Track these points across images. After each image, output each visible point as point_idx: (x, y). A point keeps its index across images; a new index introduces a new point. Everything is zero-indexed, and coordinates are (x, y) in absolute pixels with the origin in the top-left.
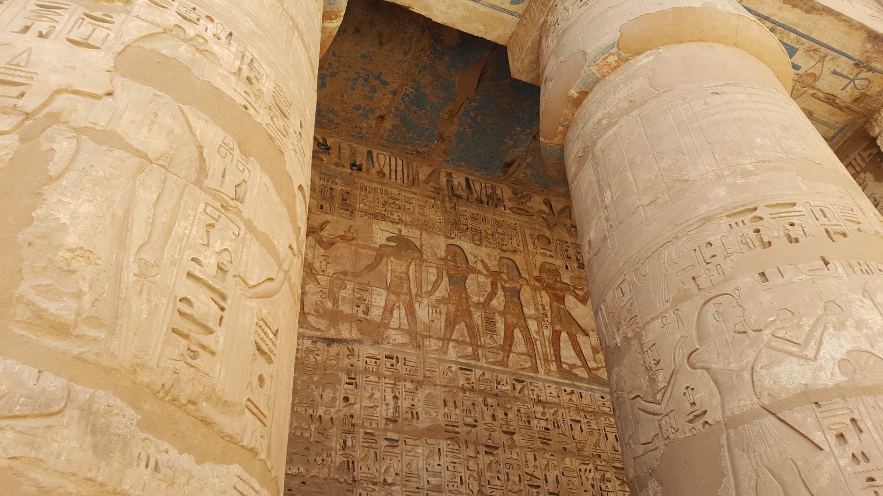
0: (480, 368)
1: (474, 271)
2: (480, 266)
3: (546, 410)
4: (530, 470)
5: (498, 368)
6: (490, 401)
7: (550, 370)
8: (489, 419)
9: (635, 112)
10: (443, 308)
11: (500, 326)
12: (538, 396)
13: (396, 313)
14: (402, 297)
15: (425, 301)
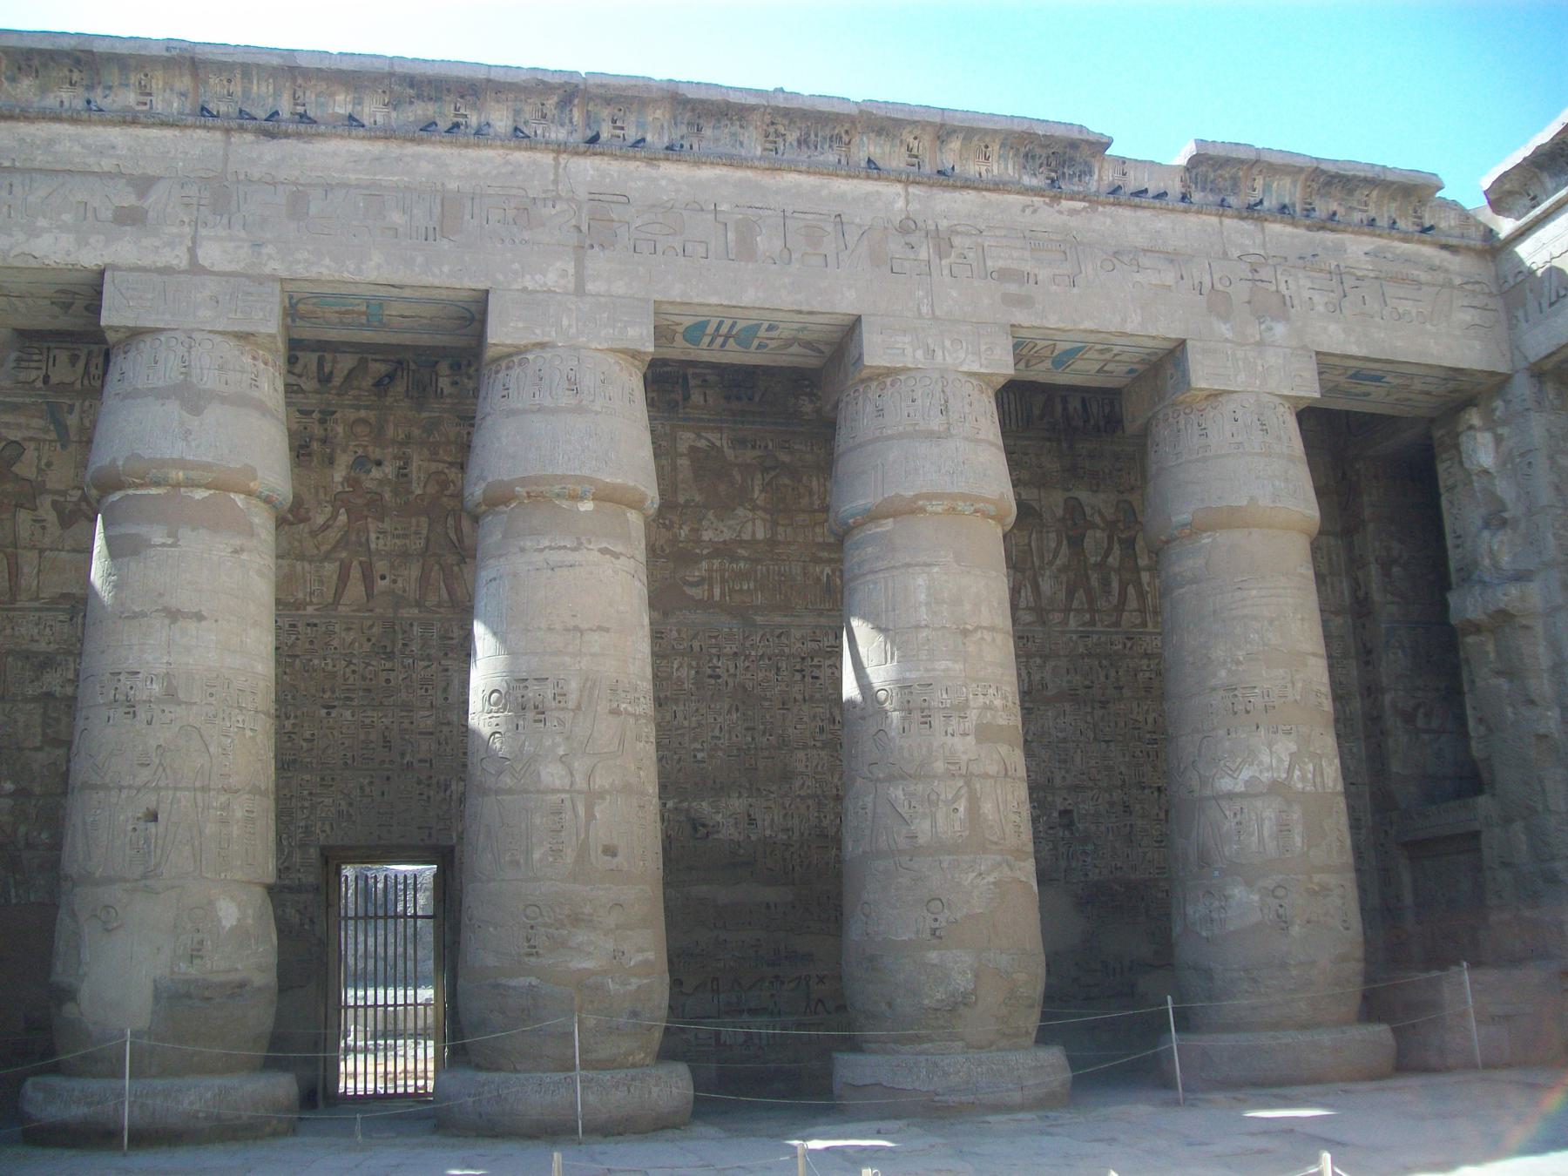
0: (1097, 633)
1: (1094, 526)
2: (1097, 519)
3: (1151, 662)
4: (1134, 716)
5: (1113, 630)
6: (1104, 662)
7: (1157, 622)
8: (1102, 679)
9: (1194, 586)
10: (1064, 578)
11: (1115, 585)
12: (1145, 650)
13: (1023, 594)
14: (1027, 574)
15: (1048, 573)
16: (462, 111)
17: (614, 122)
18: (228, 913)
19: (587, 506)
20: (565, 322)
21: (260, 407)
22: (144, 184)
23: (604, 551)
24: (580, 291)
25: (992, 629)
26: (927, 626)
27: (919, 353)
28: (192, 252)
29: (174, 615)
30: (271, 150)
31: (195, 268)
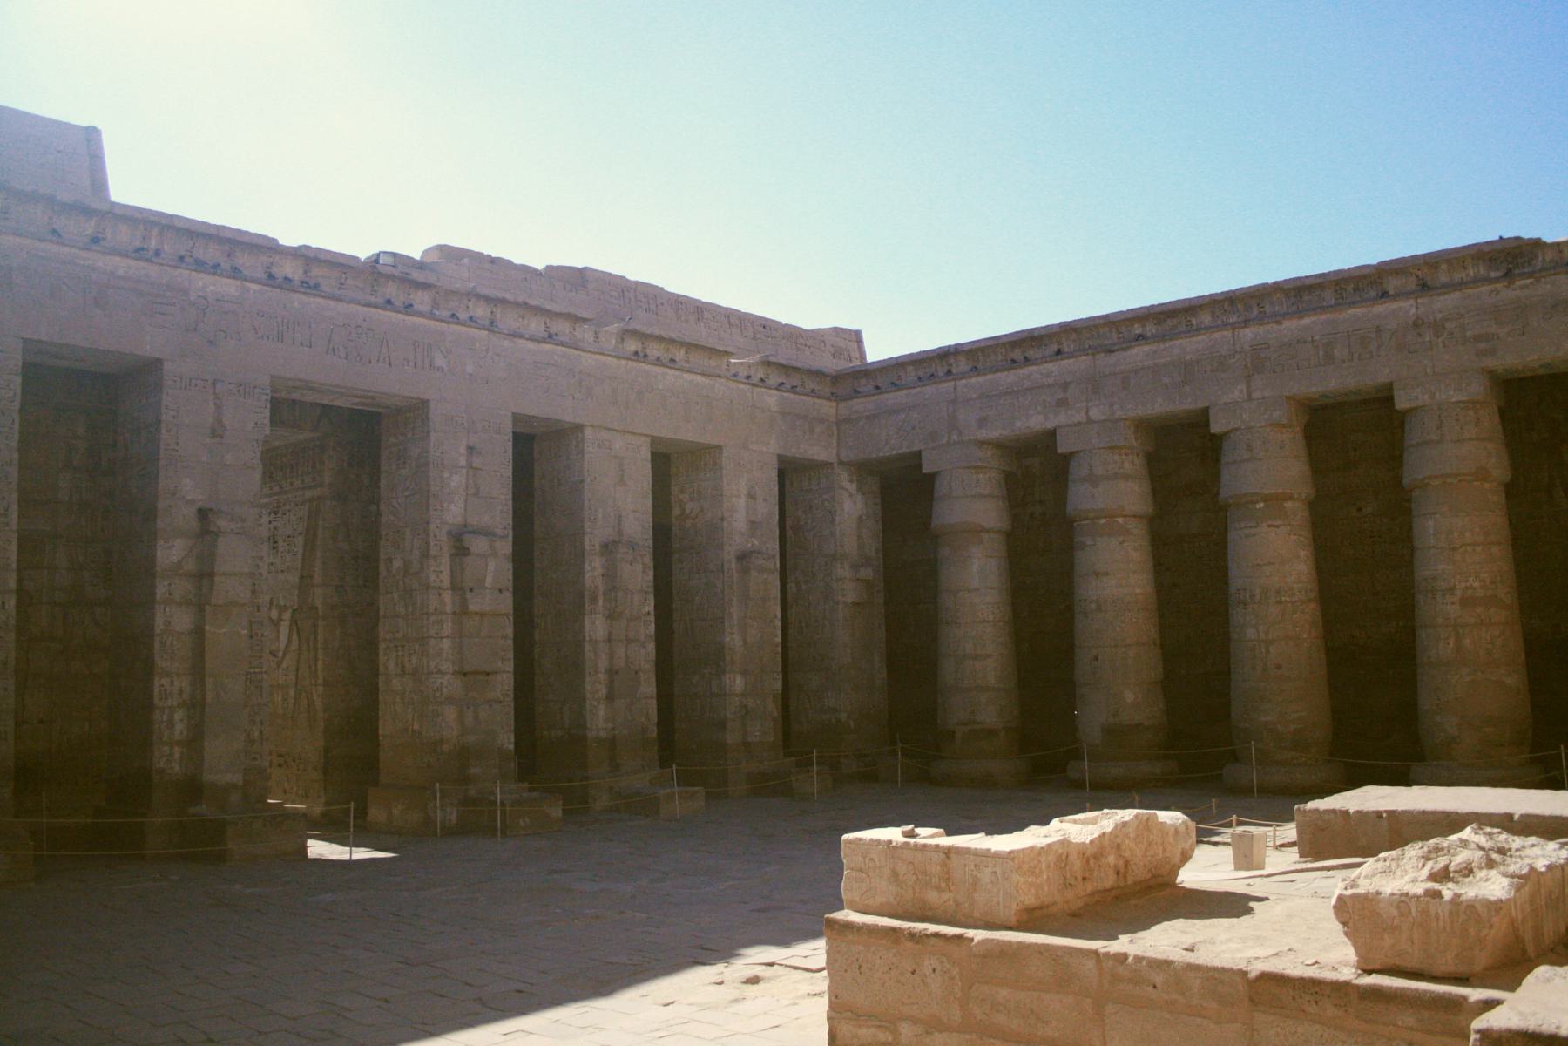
16: (1189, 319)
17: (1258, 305)
18: (1129, 697)
19: (1261, 505)
20: (1244, 416)
21: (1126, 477)
22: (1065, 386)
23: (1269, 526)
24: (1250, 398)
25: (1475, 544)
26: (1433, 547)
27: (1426, 397)
28: (1087, 413)
29: (1097, 574)
30: (1112, 359)
31: (1090, 421)
